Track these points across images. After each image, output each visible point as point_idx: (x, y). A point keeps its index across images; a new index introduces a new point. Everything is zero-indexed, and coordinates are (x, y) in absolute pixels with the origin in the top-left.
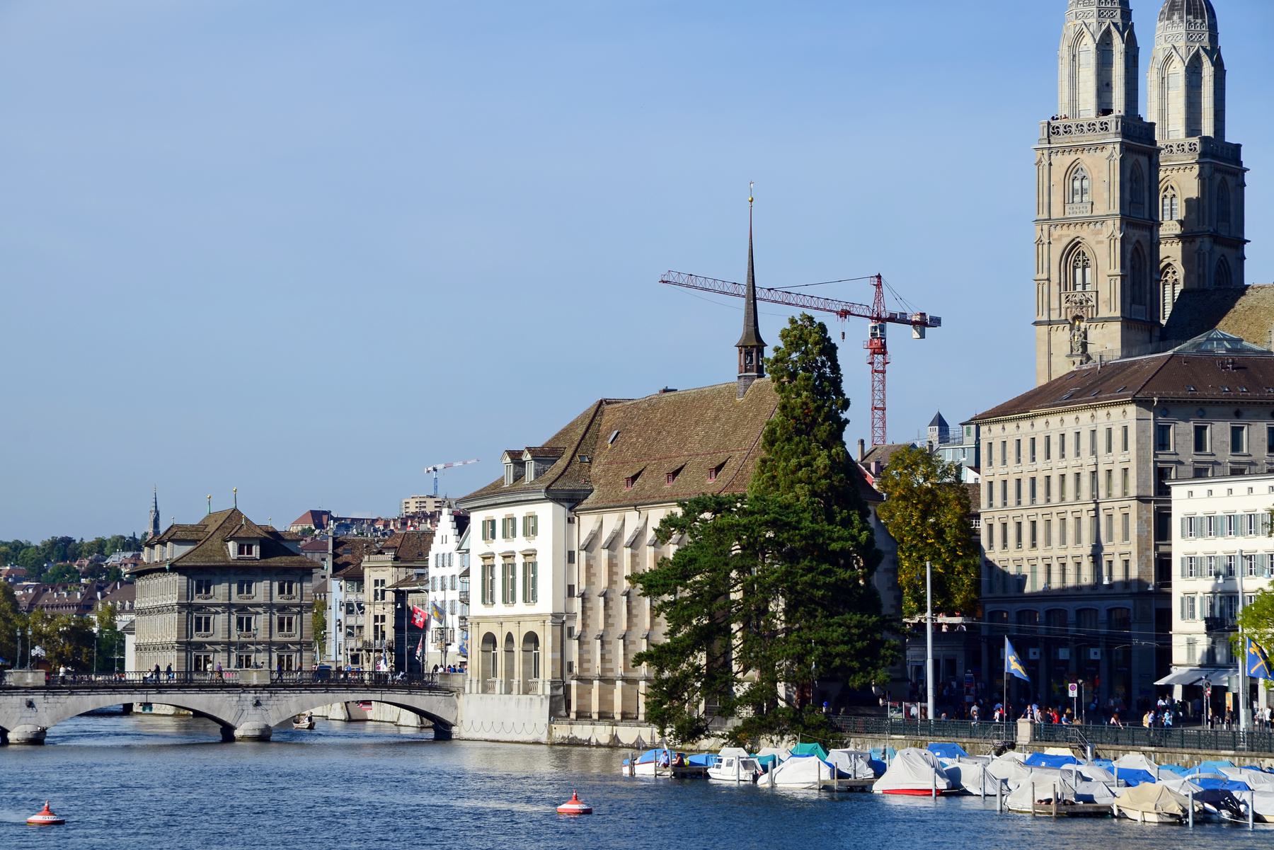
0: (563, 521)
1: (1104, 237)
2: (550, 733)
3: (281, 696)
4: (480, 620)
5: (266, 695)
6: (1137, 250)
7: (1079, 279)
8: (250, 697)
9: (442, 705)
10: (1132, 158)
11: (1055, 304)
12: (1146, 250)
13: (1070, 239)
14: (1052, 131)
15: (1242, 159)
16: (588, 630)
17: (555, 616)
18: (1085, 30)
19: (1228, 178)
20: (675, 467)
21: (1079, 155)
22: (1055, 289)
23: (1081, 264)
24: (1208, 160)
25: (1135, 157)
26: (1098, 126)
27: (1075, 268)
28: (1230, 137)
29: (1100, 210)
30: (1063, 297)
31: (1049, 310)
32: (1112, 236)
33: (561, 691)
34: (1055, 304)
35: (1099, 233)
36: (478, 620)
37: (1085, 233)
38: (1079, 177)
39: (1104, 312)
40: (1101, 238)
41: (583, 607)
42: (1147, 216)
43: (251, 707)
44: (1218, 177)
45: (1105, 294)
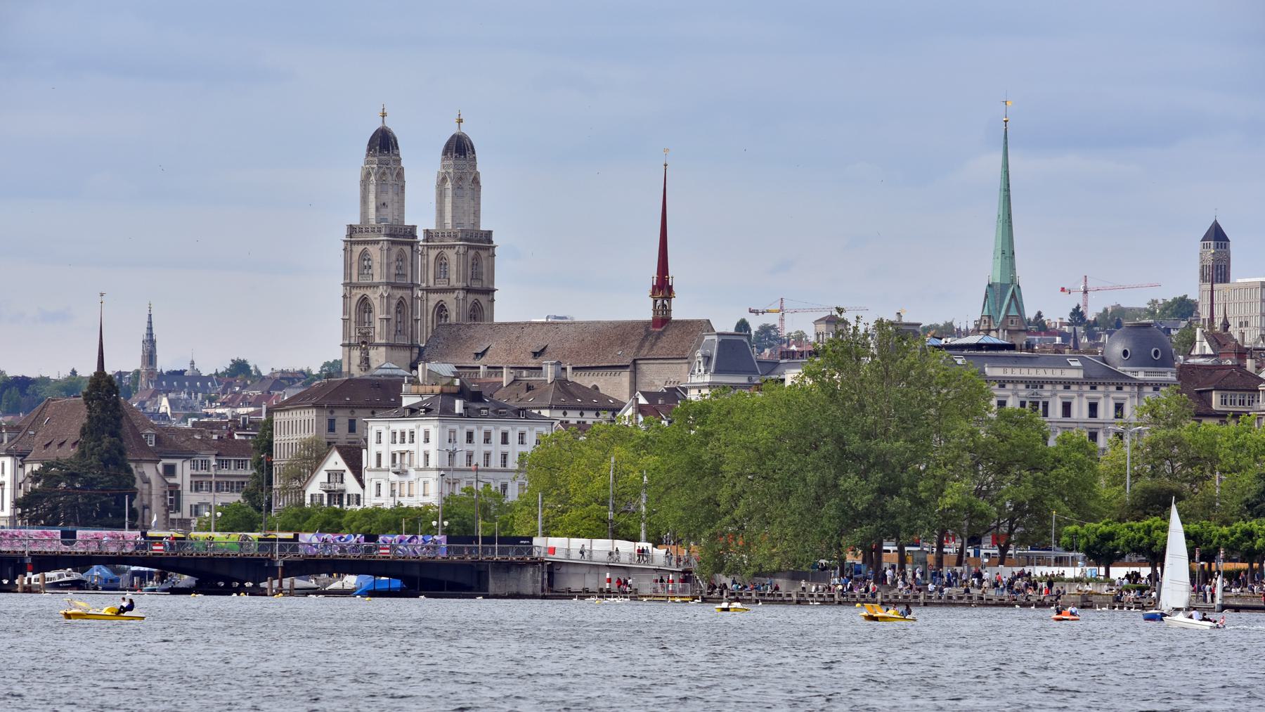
1: (377, 295)
6: (401, 303)
7: (367, 320)
10: (396, 249)
11: (353, 334)
12: (408, 302)
13: (360, 296)
14: (352, 230)
15: (494, 239)
19: (480, 252)
20: (61, 440)
22: (353, 325)
24: (461, 243)
25: (400, 247)
26: (376, 230)
27: (365, 312)
28: (484, 227)
29: (377, 279)
31: (350, 337)
32: (382, 296)
34: (353, 334)
35: (375, 293)
37: (369, 292)
39: (377, 340)
42: (409, 281)
44: (472, 253)
45: (378, 329)
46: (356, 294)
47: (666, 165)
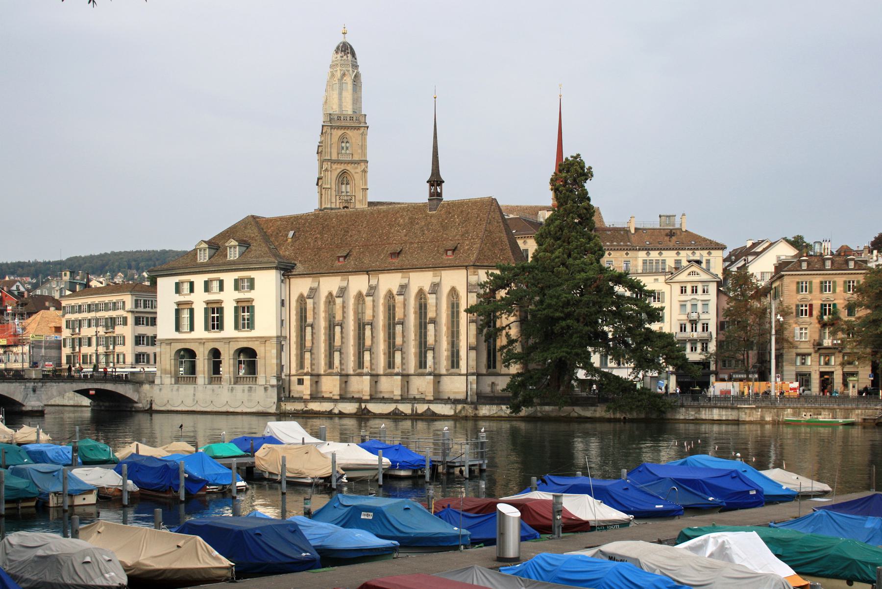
0: (279, 281)
2: (278, 407)
3: (48, 384)
4: (170, 342)
5: (40, 384)
8: (31, 385)
9: (131, 391)
11: (334, 200)
13: (340, 170)
16: (314, 346)
17: (278, 337)
18: (346, 73)
21: (345, 131)
22: (334, 193)
23: (345, 182)
30: (338, 197)
33: (281, 383)
35: (356, 168)
36: (172, 341)
37: (349, 167)
38: (345, 141)
40: (357, 171)
41: (312, 332)
43: (32, 392)
46: (336, 169)
47: (560, 96)
